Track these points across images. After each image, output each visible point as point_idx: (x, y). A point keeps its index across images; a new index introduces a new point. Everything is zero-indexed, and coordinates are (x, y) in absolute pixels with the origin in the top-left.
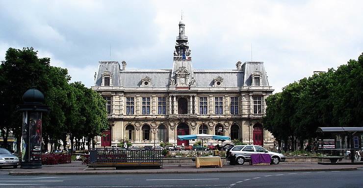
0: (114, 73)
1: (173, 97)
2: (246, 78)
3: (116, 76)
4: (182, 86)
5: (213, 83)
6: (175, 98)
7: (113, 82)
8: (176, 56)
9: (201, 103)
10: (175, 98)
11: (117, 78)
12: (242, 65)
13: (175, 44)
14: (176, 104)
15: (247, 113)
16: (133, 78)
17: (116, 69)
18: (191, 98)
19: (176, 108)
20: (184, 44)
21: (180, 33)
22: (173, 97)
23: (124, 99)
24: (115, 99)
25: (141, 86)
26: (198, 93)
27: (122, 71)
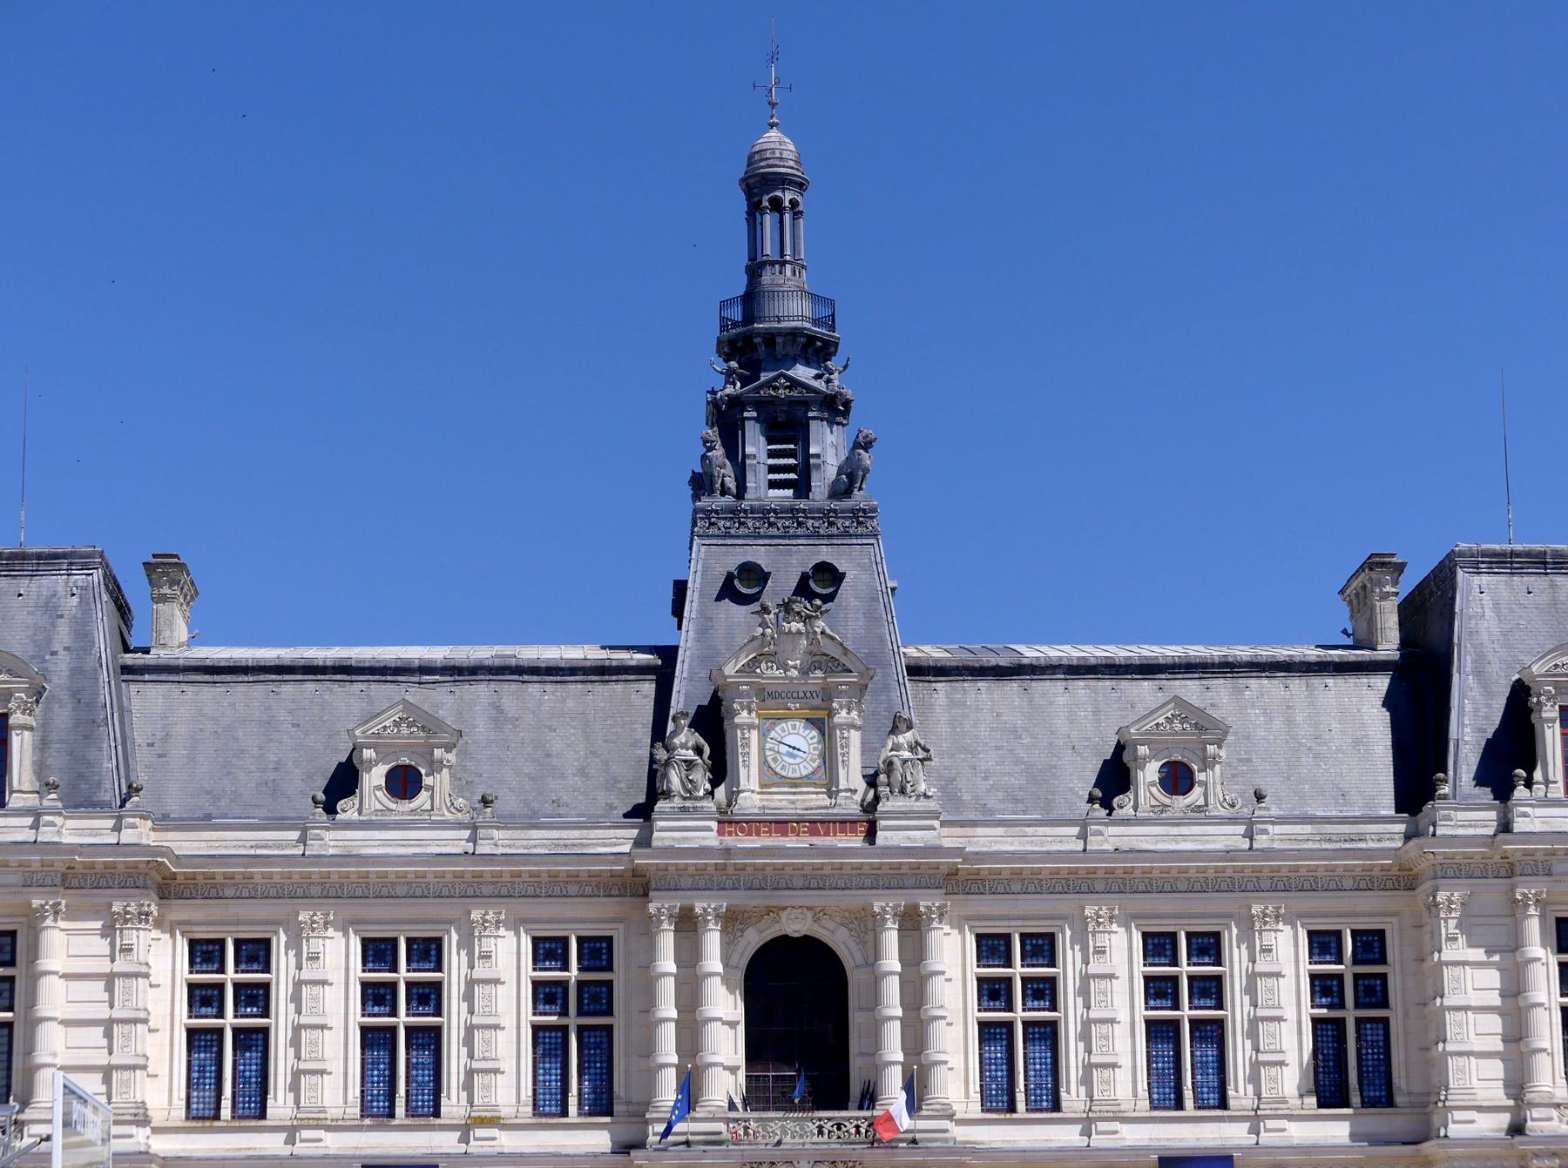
0: (61, 666)
1: (688, 925)
2: (1472, 720)
3: (82, 699)
4: (782, 802)
5: (1114, 778)
6: (713, 941)
7: (40, 768)
8: (718, 502)
9: (993, 991)
10: (713, 941)
11: (88, 724)
12: (1409, 582)
13: (711, 375)
14: (725, 1006)
15: (1496, 1093)
16: (269, 723)
17: (83, 635)
18: (891, 938)
19: (726, 1045)
20: (803, 373)
21: (755, 269)
22: (688, 925)
23: (164, 960)
24: (66, 950)
25: (348, 809)
26: (959, 880)
27: (150, 659)
